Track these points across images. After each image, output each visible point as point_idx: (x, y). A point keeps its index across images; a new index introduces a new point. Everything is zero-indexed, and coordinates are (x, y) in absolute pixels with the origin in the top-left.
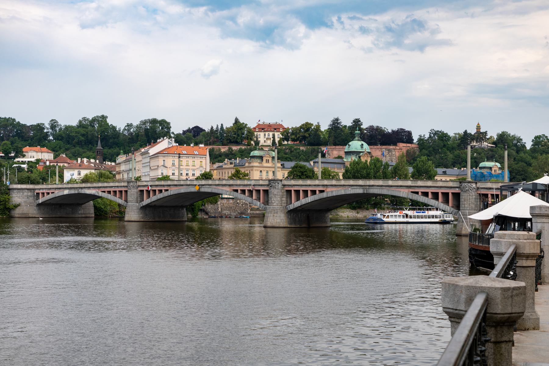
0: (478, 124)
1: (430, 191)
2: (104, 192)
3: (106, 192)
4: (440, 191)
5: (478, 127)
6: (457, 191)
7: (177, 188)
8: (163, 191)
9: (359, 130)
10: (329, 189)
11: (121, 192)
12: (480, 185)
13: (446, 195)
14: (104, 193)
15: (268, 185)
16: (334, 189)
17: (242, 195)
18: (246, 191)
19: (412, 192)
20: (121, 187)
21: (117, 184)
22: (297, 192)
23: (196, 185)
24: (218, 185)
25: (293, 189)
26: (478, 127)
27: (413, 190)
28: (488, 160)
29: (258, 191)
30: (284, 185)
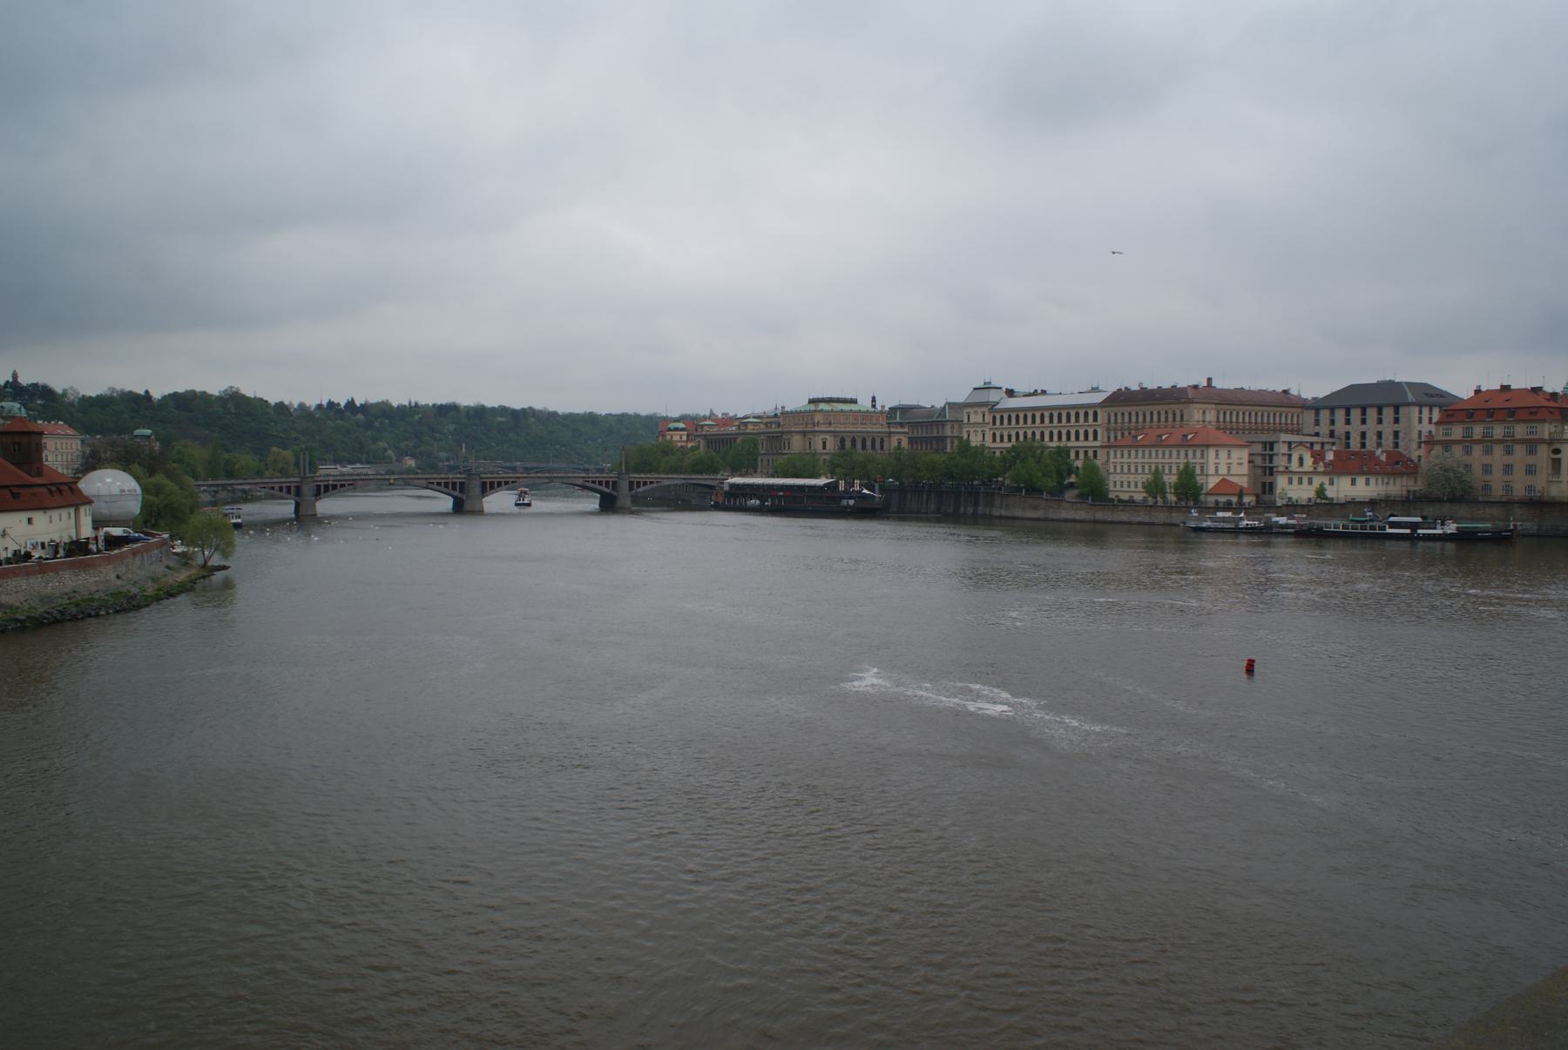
0: (15, 371)
1: (597, 480)
4: (604, 480)
5: (15, 376)
6: (616, 479)
9: (11, 388)
10: (521, 480)
11: (289, 488)
12: (631, 476)
13: (607, 483)
15: (465, 478)
20: (290, 482)
23: (389, 479)
25: (488, 481)
26: (15, 376)
28: (144, 428)
29: (454, 484)
30: (482, 478)
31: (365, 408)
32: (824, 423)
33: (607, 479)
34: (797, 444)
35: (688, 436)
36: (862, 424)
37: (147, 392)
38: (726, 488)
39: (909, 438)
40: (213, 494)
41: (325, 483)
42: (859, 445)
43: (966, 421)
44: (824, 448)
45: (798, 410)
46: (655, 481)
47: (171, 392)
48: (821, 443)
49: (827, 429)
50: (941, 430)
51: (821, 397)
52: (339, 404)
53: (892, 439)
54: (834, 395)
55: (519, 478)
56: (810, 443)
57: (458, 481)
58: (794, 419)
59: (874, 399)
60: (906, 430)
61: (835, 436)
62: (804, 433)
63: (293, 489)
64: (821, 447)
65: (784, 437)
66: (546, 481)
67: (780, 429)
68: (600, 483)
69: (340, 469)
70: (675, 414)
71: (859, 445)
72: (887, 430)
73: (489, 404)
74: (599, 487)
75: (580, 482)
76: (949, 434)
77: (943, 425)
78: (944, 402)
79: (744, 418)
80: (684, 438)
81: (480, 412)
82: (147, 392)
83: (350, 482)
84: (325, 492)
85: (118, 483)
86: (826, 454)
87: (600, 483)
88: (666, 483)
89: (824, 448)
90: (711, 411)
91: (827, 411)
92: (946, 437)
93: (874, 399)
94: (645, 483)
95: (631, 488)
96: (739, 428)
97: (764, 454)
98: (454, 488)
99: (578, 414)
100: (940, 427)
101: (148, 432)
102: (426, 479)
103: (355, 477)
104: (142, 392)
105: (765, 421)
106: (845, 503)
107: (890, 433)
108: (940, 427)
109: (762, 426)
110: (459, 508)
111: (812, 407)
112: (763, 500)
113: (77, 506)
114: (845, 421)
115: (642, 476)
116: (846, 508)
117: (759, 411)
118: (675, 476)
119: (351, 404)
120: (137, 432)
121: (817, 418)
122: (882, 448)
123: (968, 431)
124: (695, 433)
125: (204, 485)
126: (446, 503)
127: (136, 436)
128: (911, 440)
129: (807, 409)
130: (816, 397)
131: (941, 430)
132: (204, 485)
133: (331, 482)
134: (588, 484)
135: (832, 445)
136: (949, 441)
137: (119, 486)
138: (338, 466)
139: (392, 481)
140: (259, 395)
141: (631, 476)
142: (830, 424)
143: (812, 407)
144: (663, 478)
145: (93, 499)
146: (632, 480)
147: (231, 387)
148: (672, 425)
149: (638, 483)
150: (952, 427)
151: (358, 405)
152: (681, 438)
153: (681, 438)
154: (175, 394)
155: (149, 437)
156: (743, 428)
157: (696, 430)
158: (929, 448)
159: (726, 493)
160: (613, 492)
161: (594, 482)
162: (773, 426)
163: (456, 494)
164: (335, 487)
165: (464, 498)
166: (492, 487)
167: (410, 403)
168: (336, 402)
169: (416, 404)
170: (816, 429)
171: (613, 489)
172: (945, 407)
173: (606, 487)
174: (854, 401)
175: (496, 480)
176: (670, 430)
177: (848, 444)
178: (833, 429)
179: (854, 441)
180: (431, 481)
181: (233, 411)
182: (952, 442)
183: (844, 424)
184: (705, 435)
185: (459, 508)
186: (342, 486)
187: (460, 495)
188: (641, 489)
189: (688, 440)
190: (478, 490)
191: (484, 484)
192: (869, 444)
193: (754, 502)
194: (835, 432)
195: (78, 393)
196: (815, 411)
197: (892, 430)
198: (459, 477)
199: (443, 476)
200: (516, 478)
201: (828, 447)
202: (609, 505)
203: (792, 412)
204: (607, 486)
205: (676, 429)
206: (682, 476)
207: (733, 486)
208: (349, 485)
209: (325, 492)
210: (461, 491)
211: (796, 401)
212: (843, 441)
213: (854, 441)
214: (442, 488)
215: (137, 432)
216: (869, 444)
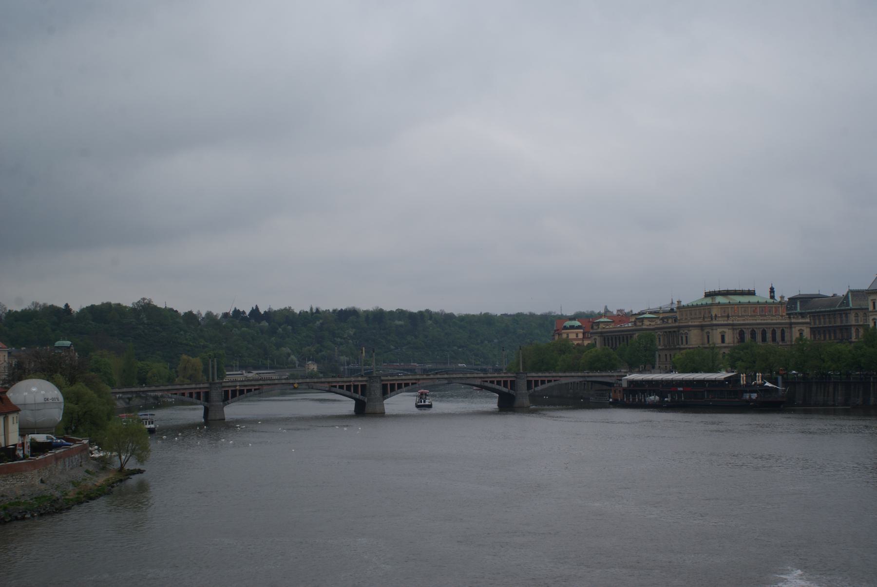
1: (495, 380)
2: (176, 394)
3: (178, 394)
7: (270, 387)
8: (253, 390)
10: (421, 382)
12: (528, 375)
13: (505, 383)
14: (175, 396)
15: (366, 381)
16: (424, 381)
17: (341, 390)
18: (345, 387)
19: (483, 381)
20: (200, 388)
21: (178, 387)
22: (392, 386)
23: (293, 384)
24: (317, 382)
25: (389, 383)
27: (483, 380)
28: (64, 339)
29: (356, 387)
30: (382, 380)
31: (269, 315)
32: (722, 317)
33: (505, 379)
34: (695, 338)
35: (584, 333)
36: (761, 316)
37: (67, 305)
38: (625, 385)
39: (811, 328)
40: (127, 401)
41: (233, 389)
42: (759, 338)
43: (871, 308)
44: (723, 341)
45: (695, 304)
46: (553, 379)
47: (89, 305)
48: (719, 337)
49: (725, 322)
50: (844, 318)
51: (717, 289)
52: (244, 312)
53: (793, 329)
54: (731, 288)
55: (419, 379)
56: (708, 337)
57: (360, 384)
58: (691, 314)
59: (772, 290)
60: (808, 320)
61: (733, 329)
62: (702, 327)
63: (202, 395)
64: (719, 340)
65: (682, 331)
66: (446, 382)
67: (677, 324)
68: (499, 383)
69: (245, 374)
70: (570, 313)
71: (759, 338)
72: (787, 321)
73: (387, 308)
74: (497, 387)
75: (478, 382)
76: (853, 323)
77: (846, 314)
78: (847, 290)
79: (640, 314)
80: (581, 336)
81: (378, 316)
82: (67, 305)
83: (257, 387)
84: (232, 398)
85: (43, 392)
86: (725, 347)
87: (499, 383)
88: (564, 381)
89: (723, 341)
90: (606, 307)
91: (724, 304)
92: (851, 326)
93: (772, 290)
94: (543, 382)
95: (529, 386)
96: (635, 324)
97: (661, 350)
98: (356, 391)
99: (473, 315)
100: (844, 315)
101: (67, 343)
102: (329, 382)
103: (261, 382)
104: (62, 305)
105: (661, 316)
106: (748, 397)
107: (791, 324)
108: (844, 315)
109: (659, 322)
110: (361, 411)
111: (709, 301)
112: (662, 396)
113: (5, 415)
114: (743, 314)
115: (540, 374)
116: (748, 401)
117: (654, 306)
118: (573, 374)
119: (255, 312)
120: (58, 344)
121: (715, 311)
122: (783, 339)
123: (874, 319)
124: (591, 331)
125: (119, 393)
126: (348, 406)
127: (58, 347)
128: (813, 331)
129: (704, 302)
130: (712, 290)
131: (844, 318)
132: (119, 393)
133: (238, 388)
134: (486, 384)
135: (731, 338)
136: (853, 330)
137: (44, 395)
138: (244, 372)
139: (296, 385)
140: (169, 306)
141: (528, 375)
142: (728, 317)
143: (709, 301)
144: (561, 377)
145: (19, 407)
146: (529, 379)
147: (144, 299)
148: (568, 323)
149: (536, 382)
150: (857, 316)
151: (262, 313)
152: (577, 336)
153: (577, 336)
154: (93, 306)
155: (68, 348)
156: (638, 324)
157: (592, 328)
158: (833, 338)
159: (624, 389)
160: (512, 392)
161: (492, 382)
162: (670, 321)
163: (357, 396)
164: (242, 392)
165: (366, 401)
166: (392, 389)
167: (311, 309)
168: (241, 310)
169: (317, 310)
170: (714, 322)
171: (511, 389)
172: (847, 296)
173: (504, 386)
174: (751, 293)
175: (396, 382)
176: (565, 328)
177: (748, 337)
178: (730, 322)
179: (753, 334)
180: (333, 385)
181: (146, 322)
182: (857, 331)
183: (742, 316)
184: (601, 333)
185: (361, 411)
186: (249, 391)
187: (361, 398)
188: (540, 388)
189: (584, 337)
190: (378, 392)
191: (384, 387)
192: (769, 335)
193: (654, 398)
194: (733, 325)
195: (5, 309)
196: (712, 305)
197: (793, 321)
198: (360, 380)
199: (345, 379)
200: (416, 379)
201: (727, 339)
202: (507, 405)
203: (688, 306)
204: (505, 385)
205: (572, 327)
206: (580, 374)
207: (631, 382)
208: (255, 390)
209: (232, 398)
210: (363, 394)
211: (693, 296)
212: (742, 334)
213: (753, 334)
214: (344, 391)
215: (58, 344)
216: (769, 335)
